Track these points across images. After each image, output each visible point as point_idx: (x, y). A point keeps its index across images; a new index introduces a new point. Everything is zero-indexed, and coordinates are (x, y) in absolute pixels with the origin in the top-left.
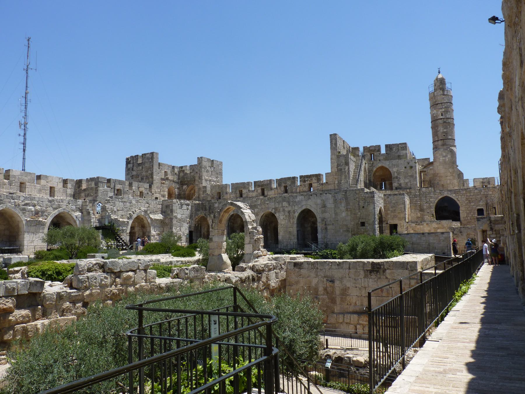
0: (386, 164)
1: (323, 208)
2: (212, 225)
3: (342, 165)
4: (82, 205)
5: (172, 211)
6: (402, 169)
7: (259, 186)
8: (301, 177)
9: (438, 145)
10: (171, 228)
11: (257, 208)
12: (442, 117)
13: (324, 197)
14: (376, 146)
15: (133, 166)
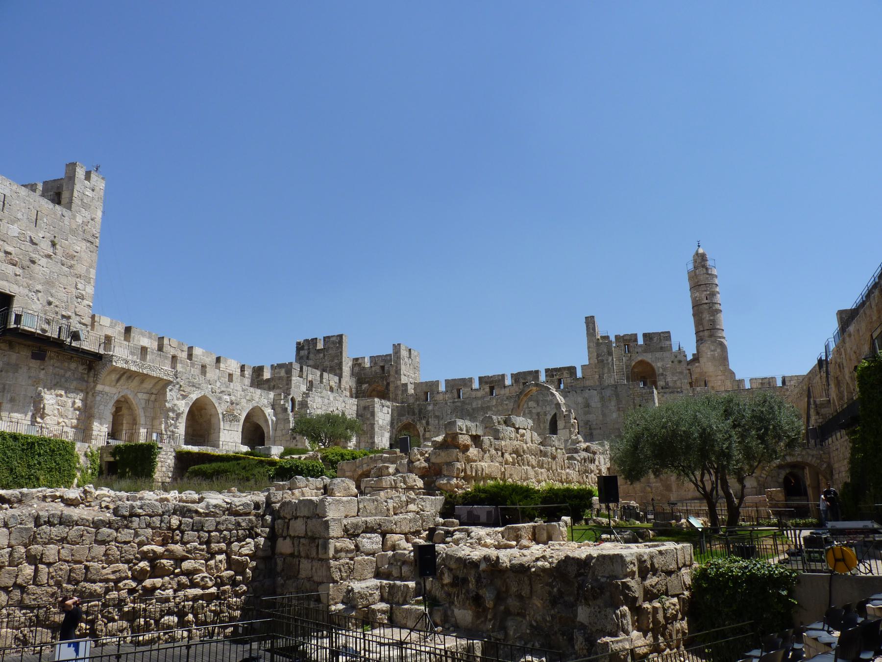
0: (648, 357)
1: (586, 407)
2: (424, 435)
3: (604, 355)
4: (274, 399)
5: (373, 414)
6: (667, 364)
7: (486, 383)
8: (547, 370)
9: (704, 336)
10: (372, 437)
11: (492, 410)
12: (707, 301)
13: (587, 393)
14: (631, 334)
15: (309, 353)
